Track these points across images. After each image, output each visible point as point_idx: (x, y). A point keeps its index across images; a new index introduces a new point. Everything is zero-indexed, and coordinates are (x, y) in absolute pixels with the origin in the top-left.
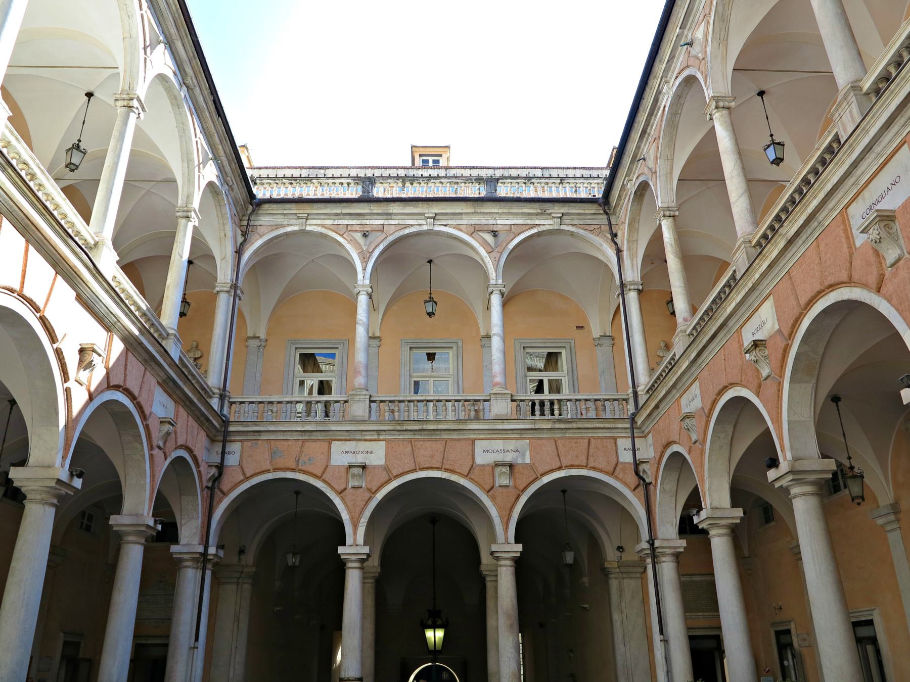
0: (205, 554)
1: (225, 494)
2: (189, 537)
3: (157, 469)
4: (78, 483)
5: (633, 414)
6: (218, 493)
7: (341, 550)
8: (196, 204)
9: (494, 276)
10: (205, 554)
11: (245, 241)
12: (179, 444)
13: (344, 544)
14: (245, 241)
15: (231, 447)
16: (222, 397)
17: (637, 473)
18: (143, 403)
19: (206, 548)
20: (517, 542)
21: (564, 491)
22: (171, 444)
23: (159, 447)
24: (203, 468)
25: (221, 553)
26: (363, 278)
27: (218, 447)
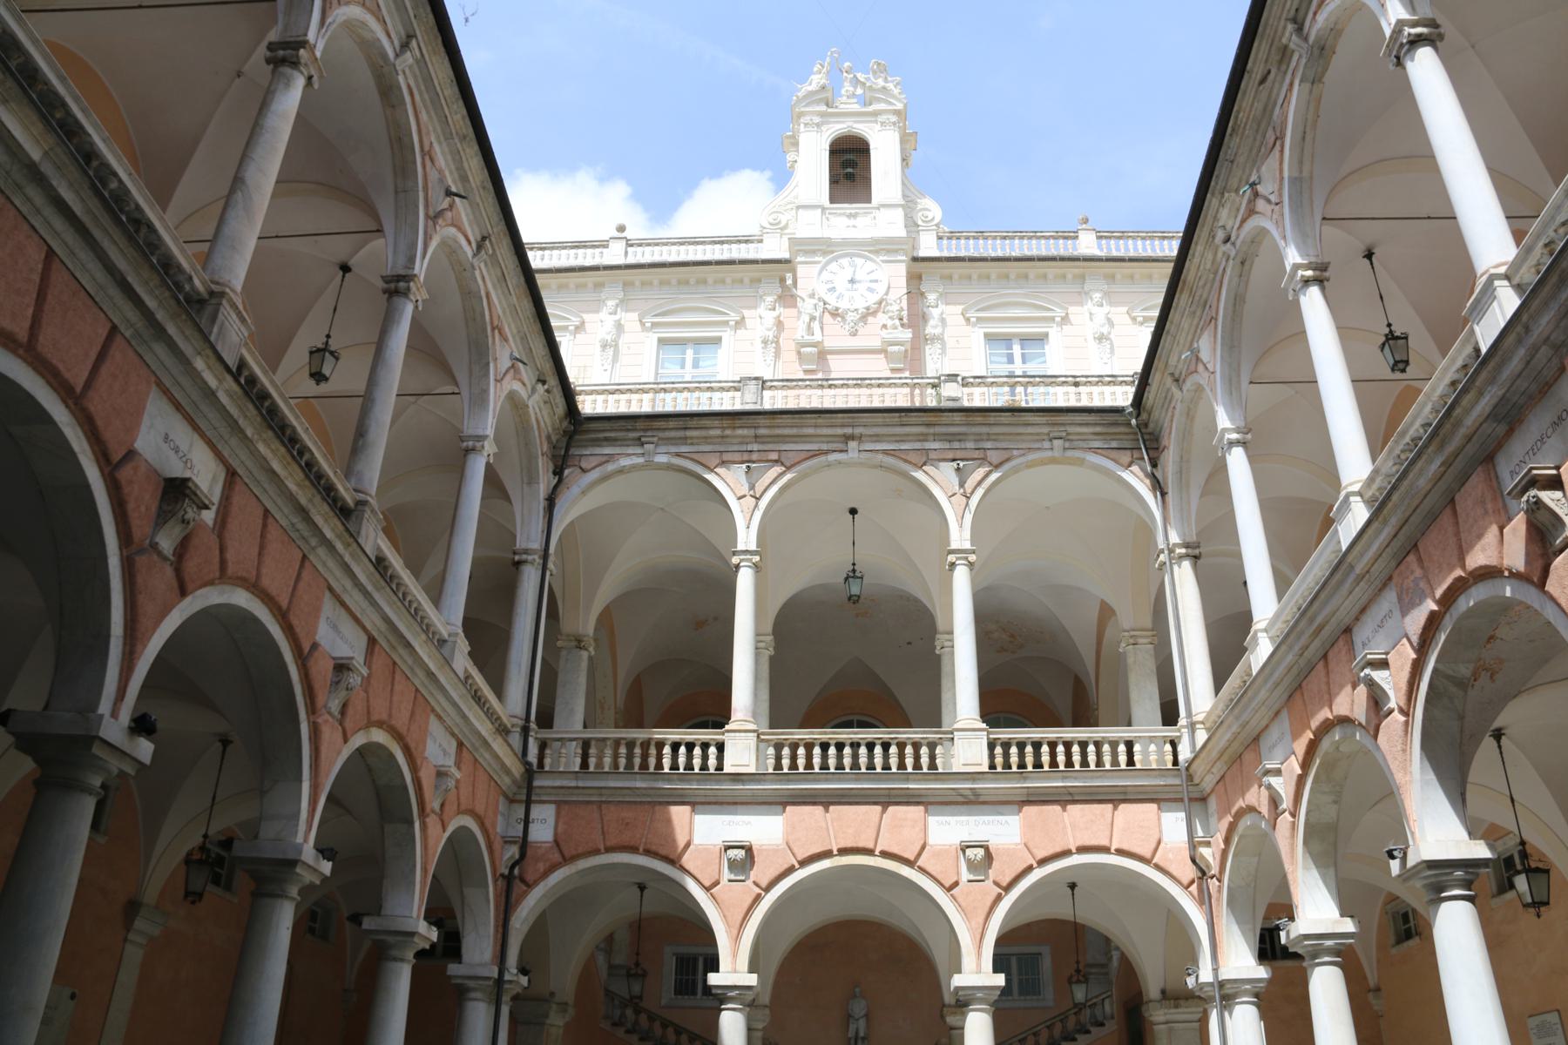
0: (500, 981)
1: (530, 886)
2: (478, 951)
3: (431, 842)
4: (326, 867)
5: (1191, 763)
6: (518, 887)
7: (713, 979)
8: (490, 432)
9: (960, 537)
10: (500, 981)
11: (560, 481)
12: (463, 807)
13: (717, 971)
14: (560, 481)
15: (537, 812)
16: (525, 731)
17: (1193, 861)
18: (412, 746)
19: (501, 973)
20: (996, 970)
21: (1073, 886)
22: (451, 808)
23: (433, 811)
24: (497, 845)
25: (524, 980)
26: (747, 538)
27: (520, 811)
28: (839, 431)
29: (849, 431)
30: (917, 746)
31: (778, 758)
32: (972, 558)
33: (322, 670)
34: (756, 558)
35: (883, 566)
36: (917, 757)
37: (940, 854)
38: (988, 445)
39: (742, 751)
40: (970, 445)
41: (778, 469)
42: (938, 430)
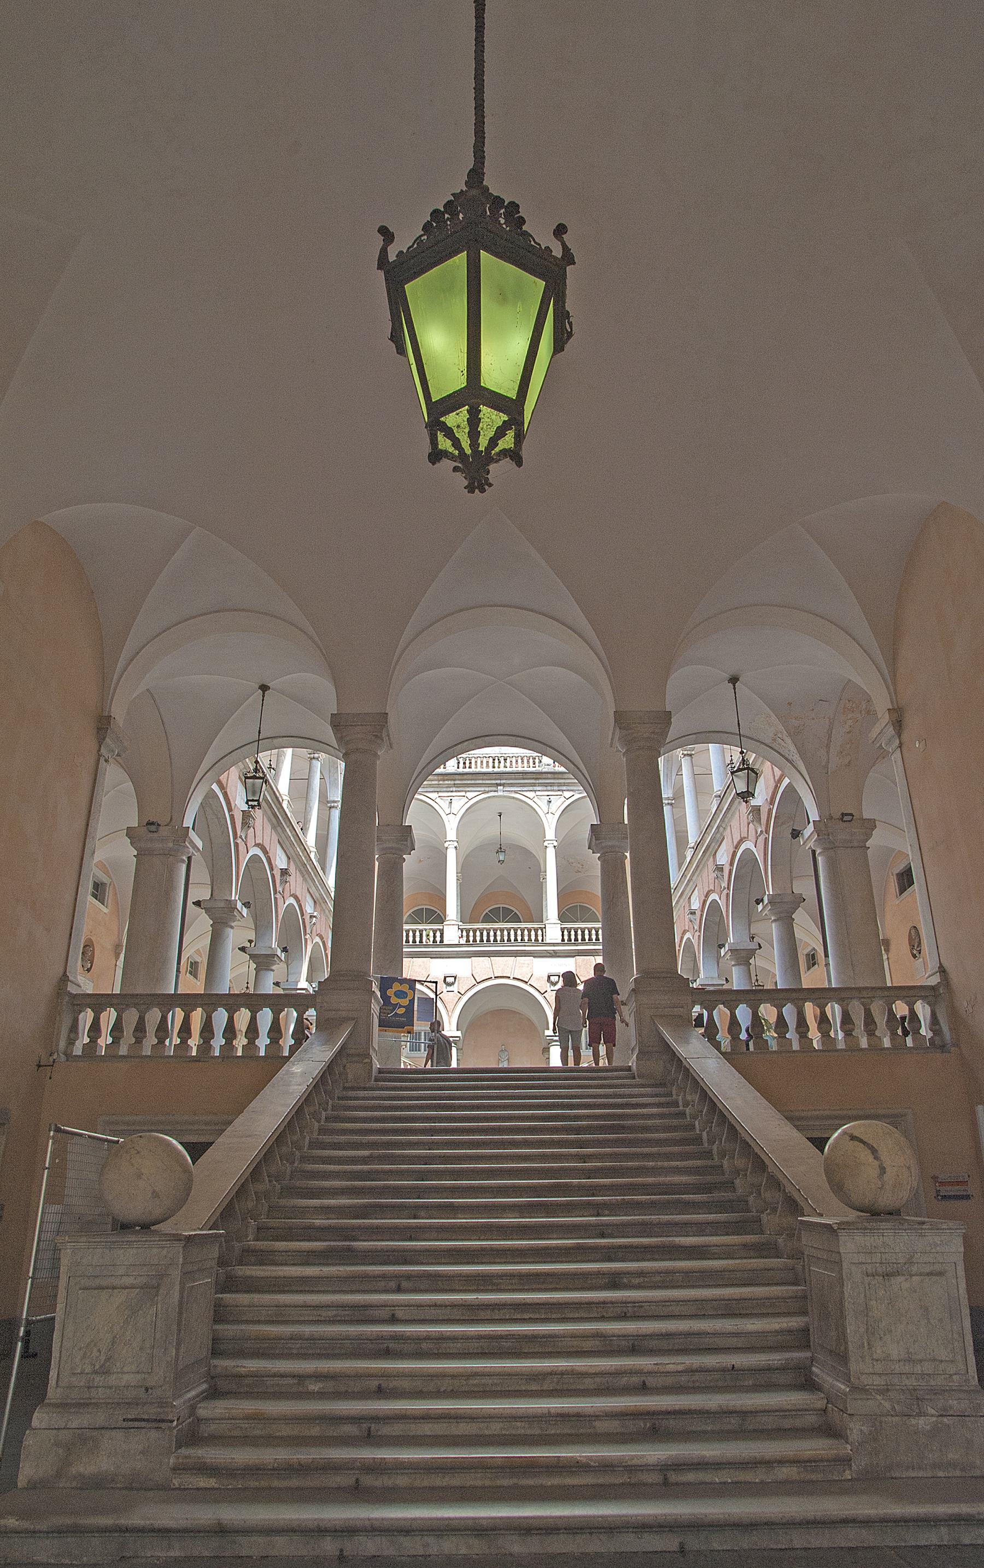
8: (339, 799)
9: (550, 834)
26: (451, 834)
28: (494, 782)
29: (498, 782)
30: (529, 931)
31: (468, 936)
32: (556, 844)
33: (307, 918)
34: (456, 844)
35: (514, 832)
36: (529, 935)
37: (538, 979)
38: (564, 788)
39: (452, 934)
40: (556, 788)
41: (465, 800)
42: (541, 781)
